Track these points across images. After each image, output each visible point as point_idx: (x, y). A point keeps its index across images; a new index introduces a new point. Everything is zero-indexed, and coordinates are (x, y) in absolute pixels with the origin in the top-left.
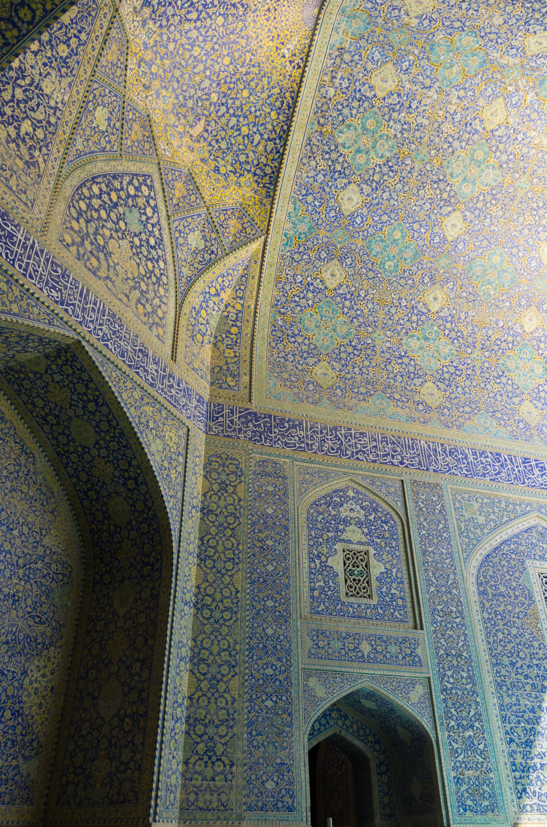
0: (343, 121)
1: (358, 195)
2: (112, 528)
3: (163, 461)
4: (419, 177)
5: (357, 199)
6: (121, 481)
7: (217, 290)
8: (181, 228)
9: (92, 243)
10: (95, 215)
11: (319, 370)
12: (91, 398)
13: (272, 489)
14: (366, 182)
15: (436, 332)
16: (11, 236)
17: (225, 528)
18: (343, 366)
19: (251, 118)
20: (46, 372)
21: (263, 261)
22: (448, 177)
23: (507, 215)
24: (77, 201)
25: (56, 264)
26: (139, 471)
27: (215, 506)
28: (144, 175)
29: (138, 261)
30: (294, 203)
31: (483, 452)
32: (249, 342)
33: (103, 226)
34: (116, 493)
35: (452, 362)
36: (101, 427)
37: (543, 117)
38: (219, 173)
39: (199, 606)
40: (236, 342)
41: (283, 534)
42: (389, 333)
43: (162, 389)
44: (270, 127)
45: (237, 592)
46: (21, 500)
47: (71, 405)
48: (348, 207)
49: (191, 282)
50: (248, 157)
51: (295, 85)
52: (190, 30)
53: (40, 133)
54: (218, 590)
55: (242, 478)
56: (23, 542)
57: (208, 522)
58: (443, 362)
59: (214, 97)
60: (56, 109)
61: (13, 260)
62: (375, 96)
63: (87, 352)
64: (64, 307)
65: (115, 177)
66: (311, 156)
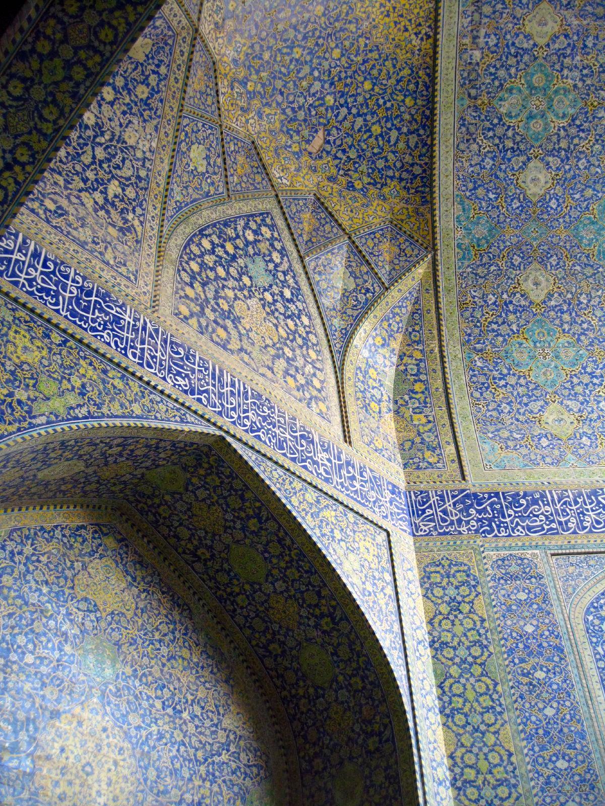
0: (501, 85)
1: (544, 172)
2: (311, 690)
3: (364, 583)
5: (544, 177)
6: (312, 623)
9: (214, 310)
10: (212, 275)
11: (550, 416)
12: (251, 513)
13: (525, 597)
14: (550, 153)
16: (117, 320)
17: (471, 665)
18: (582, 403)
19: (381, 113)
20: (187, 490)
21: (436, 287)
24: (187, 263)
25: (176, 344)
26: (334, 603)
27: (449, 635)
28: (262, 214)
29: (275, 321)
30: (461, 203)
32: (443, 399)
33: (224, 286)
34: (308, 640)
36: (271, 550)
38: (355, 190)
39: (459, 784)
40: (425, 403)
41: (556, 659)
43: (342, 484)
44: (407, 117)
45: (510, 755)
46: (184, 669)
47: (226, 528)
48: (534, 191)
49: (348, 336)
50: (387, 161)
51: (428, 59)
54: (481, 756)
55: (479, 589)
56: (197, 727)
57: (444, 660)
59: (330, 100)
61: (125, 349)
62: (535, 45)
63: (235, 451)
64: (196, 396)
65: (226, 224)
66: (470, 138)
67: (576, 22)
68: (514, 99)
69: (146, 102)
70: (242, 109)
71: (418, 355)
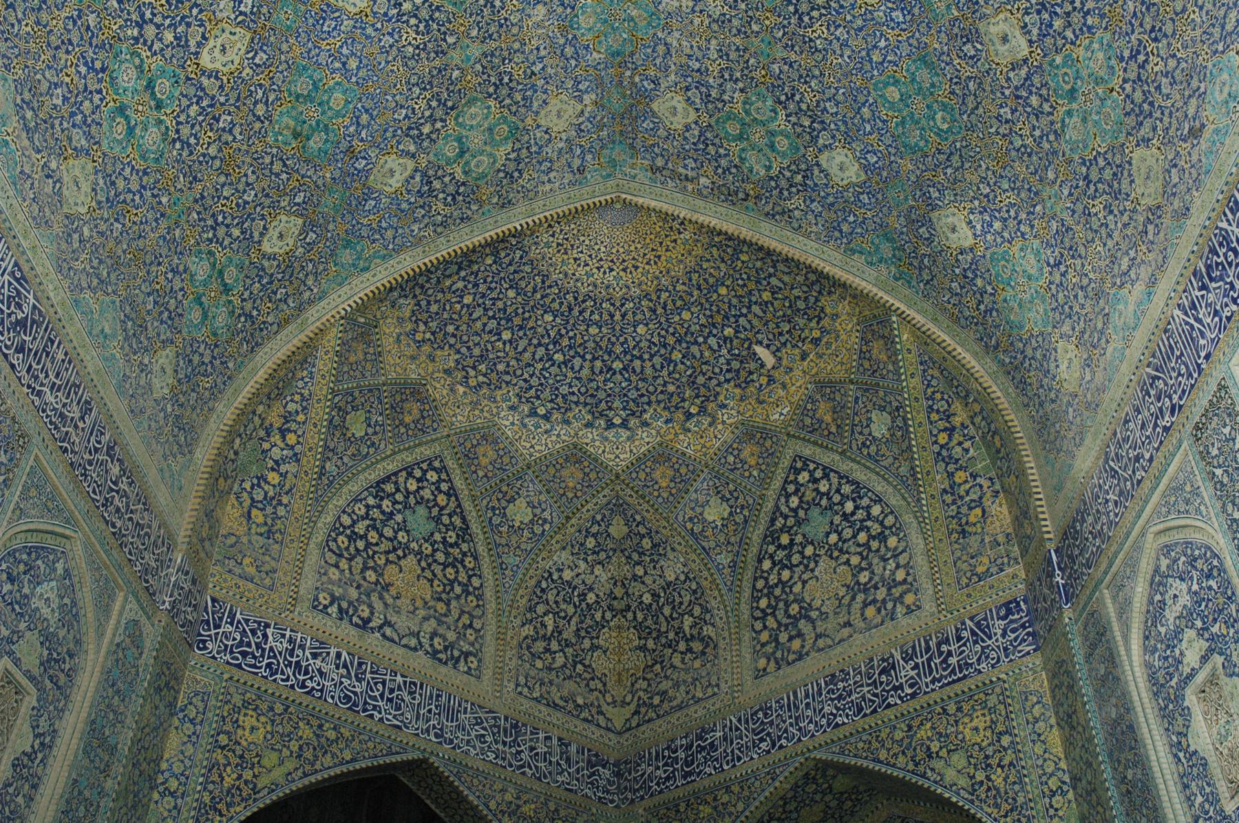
0: (736, 166)
1: (834, 153)
3: (973, 777)
4: (796, 48)
7: (945, 429)
8: (861, 438)
14: (815, 139)
15: (1065, 64)
19: (752, 285)
30: (853, 251)
35: (1122, 59)
38: (819, 339)
42: (1051, 175)
43: (933, 682)
44: (759, 264)
48: (853, 173)
50: (799, 297)
53: (697, 611)
58: (1116, 82)
59: (728, 331)
60: (687, 577)
62: (696, 123)
65: (773, 521)
67: (673, 77)
68: (752, 159)
69: (654, 546)
71: (977, 407)
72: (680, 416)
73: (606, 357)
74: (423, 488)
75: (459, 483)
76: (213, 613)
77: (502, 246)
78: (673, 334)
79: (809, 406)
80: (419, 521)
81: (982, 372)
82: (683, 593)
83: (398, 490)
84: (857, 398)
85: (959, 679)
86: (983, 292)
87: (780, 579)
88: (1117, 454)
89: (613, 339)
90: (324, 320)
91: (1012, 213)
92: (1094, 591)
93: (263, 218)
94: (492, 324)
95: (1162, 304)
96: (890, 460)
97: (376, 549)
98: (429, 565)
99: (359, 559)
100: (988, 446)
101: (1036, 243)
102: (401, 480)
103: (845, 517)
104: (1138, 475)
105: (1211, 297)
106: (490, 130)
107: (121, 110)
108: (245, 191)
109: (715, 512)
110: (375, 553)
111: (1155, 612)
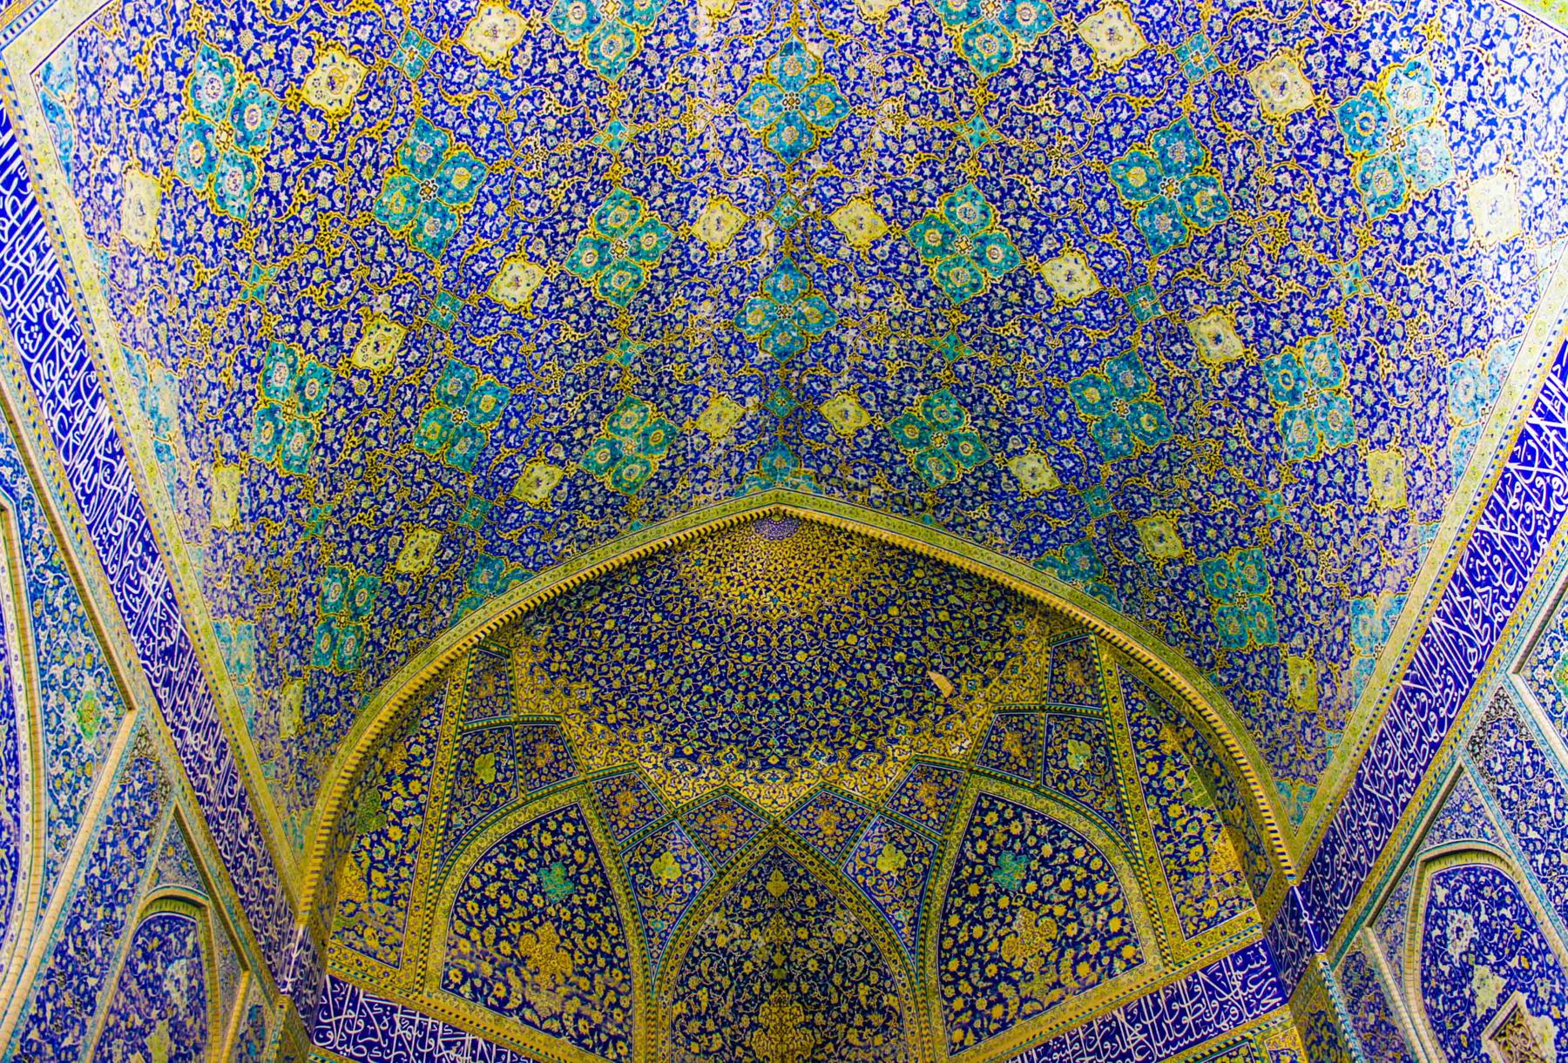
1: (1025, 459)
4: (986, 348)
7: (1154, 758)
14: (1004, 444)
19: (927, 605)
22: (979, 293)
23: (1040, 159)
30: (1044, 565)
31: (1505, 481)
35: (1348, 360)
37: (846, 126)
38: (1004, 663)
42: (1272, 479)
43: (1166, 1046)
44: (935, 581)
48: (1047, 479)
50: (981, 617)
52: (814, 697)
53: (874, 977)
58: (1343, 384)
59: (900, 656)
60: (860, 939)
62: (870, 427)
65: (958, 870)
68: (932, 464)
69: (820, 904)
70: (880, 762)
71: (1190, 732)
72: (844, 753)
73: (761, 688)
74: (559, 842)
75: (598, 837)
76: (334, 995)
77: (650, 563)
78: (837, 661)
79: (994, 738)
80: (555, 881)
81: (1194, 694)
82: (856, 957)
83: (531, 845)
84: (1050, 727)
85: (1197, 1042)
86: (1195, 605)
87: (971, 937)
88: (1372, 776)
89: (770, 668)
90: (454, 649)
91: (1228, 520)
92: (1353, 931)
93: (400, 533)
94: (635, 652)
95: (1417, 611)
96: (1092, 795)
97: (509, 915)
98: (569, 933)
99: (491, 929)
100: (1206, 775)
101: (1257, 551)
102: (534, 833)
103: (1044, 861)
104: (1402, 798)
105: (1478, 603)
106: (645, 434)
107: (272, 412)
108: (384, 503)
109: (890, 862)
110: (509, 920)
111: (1434, 950)
